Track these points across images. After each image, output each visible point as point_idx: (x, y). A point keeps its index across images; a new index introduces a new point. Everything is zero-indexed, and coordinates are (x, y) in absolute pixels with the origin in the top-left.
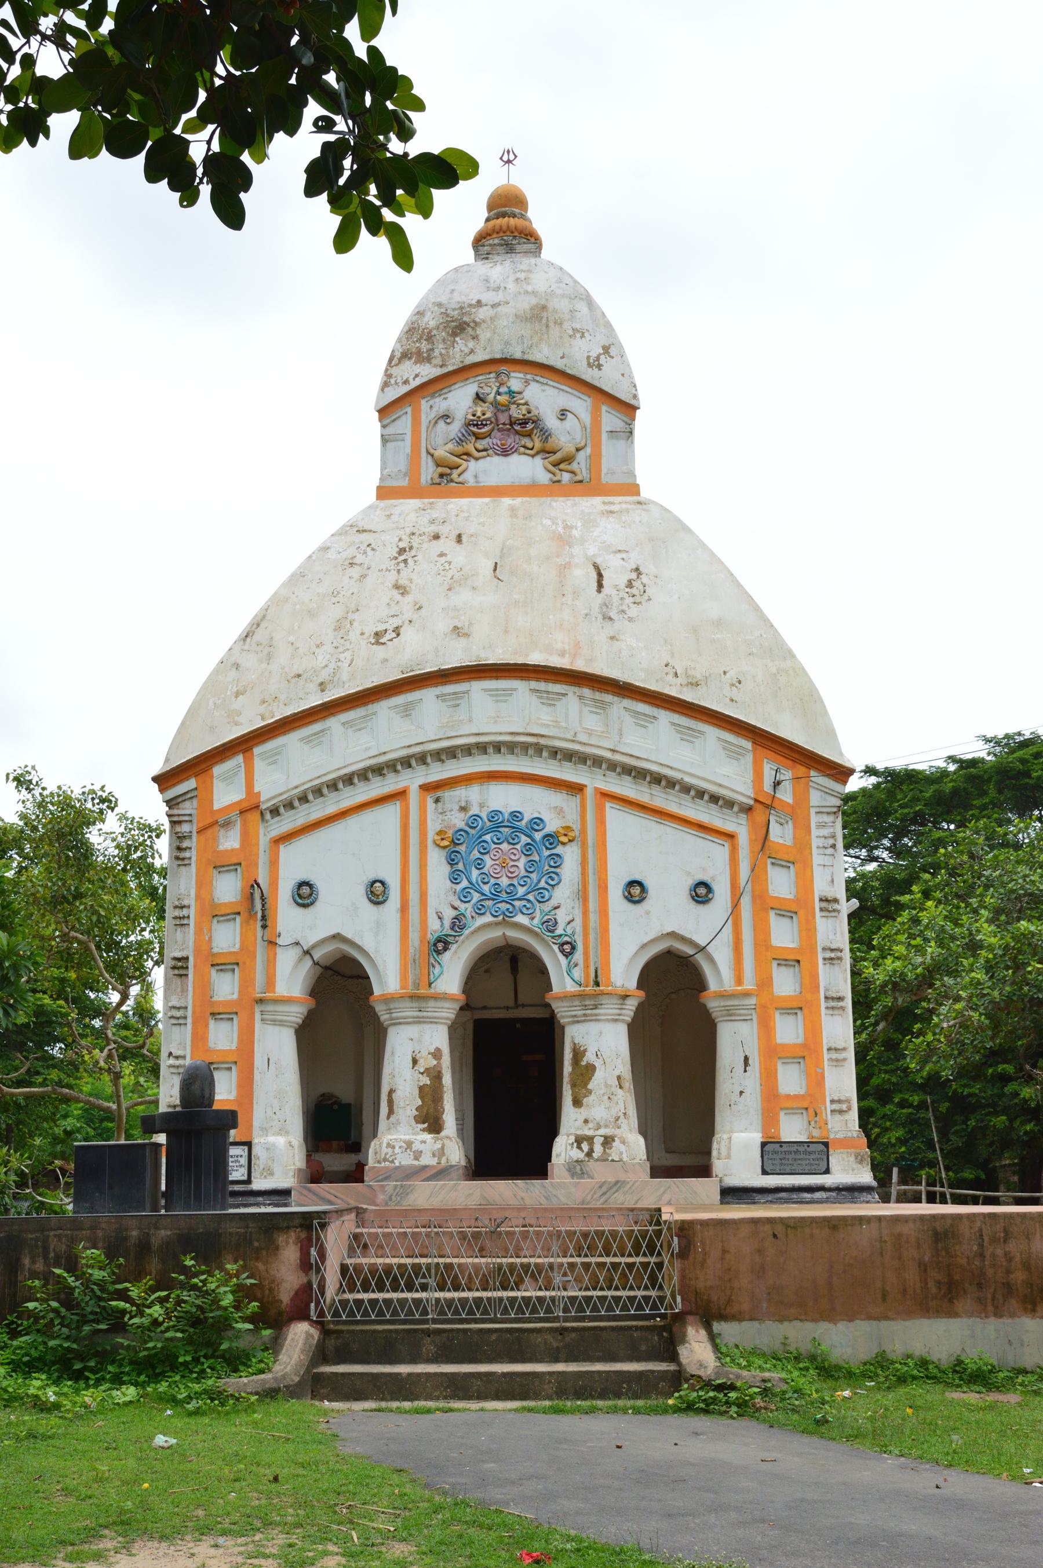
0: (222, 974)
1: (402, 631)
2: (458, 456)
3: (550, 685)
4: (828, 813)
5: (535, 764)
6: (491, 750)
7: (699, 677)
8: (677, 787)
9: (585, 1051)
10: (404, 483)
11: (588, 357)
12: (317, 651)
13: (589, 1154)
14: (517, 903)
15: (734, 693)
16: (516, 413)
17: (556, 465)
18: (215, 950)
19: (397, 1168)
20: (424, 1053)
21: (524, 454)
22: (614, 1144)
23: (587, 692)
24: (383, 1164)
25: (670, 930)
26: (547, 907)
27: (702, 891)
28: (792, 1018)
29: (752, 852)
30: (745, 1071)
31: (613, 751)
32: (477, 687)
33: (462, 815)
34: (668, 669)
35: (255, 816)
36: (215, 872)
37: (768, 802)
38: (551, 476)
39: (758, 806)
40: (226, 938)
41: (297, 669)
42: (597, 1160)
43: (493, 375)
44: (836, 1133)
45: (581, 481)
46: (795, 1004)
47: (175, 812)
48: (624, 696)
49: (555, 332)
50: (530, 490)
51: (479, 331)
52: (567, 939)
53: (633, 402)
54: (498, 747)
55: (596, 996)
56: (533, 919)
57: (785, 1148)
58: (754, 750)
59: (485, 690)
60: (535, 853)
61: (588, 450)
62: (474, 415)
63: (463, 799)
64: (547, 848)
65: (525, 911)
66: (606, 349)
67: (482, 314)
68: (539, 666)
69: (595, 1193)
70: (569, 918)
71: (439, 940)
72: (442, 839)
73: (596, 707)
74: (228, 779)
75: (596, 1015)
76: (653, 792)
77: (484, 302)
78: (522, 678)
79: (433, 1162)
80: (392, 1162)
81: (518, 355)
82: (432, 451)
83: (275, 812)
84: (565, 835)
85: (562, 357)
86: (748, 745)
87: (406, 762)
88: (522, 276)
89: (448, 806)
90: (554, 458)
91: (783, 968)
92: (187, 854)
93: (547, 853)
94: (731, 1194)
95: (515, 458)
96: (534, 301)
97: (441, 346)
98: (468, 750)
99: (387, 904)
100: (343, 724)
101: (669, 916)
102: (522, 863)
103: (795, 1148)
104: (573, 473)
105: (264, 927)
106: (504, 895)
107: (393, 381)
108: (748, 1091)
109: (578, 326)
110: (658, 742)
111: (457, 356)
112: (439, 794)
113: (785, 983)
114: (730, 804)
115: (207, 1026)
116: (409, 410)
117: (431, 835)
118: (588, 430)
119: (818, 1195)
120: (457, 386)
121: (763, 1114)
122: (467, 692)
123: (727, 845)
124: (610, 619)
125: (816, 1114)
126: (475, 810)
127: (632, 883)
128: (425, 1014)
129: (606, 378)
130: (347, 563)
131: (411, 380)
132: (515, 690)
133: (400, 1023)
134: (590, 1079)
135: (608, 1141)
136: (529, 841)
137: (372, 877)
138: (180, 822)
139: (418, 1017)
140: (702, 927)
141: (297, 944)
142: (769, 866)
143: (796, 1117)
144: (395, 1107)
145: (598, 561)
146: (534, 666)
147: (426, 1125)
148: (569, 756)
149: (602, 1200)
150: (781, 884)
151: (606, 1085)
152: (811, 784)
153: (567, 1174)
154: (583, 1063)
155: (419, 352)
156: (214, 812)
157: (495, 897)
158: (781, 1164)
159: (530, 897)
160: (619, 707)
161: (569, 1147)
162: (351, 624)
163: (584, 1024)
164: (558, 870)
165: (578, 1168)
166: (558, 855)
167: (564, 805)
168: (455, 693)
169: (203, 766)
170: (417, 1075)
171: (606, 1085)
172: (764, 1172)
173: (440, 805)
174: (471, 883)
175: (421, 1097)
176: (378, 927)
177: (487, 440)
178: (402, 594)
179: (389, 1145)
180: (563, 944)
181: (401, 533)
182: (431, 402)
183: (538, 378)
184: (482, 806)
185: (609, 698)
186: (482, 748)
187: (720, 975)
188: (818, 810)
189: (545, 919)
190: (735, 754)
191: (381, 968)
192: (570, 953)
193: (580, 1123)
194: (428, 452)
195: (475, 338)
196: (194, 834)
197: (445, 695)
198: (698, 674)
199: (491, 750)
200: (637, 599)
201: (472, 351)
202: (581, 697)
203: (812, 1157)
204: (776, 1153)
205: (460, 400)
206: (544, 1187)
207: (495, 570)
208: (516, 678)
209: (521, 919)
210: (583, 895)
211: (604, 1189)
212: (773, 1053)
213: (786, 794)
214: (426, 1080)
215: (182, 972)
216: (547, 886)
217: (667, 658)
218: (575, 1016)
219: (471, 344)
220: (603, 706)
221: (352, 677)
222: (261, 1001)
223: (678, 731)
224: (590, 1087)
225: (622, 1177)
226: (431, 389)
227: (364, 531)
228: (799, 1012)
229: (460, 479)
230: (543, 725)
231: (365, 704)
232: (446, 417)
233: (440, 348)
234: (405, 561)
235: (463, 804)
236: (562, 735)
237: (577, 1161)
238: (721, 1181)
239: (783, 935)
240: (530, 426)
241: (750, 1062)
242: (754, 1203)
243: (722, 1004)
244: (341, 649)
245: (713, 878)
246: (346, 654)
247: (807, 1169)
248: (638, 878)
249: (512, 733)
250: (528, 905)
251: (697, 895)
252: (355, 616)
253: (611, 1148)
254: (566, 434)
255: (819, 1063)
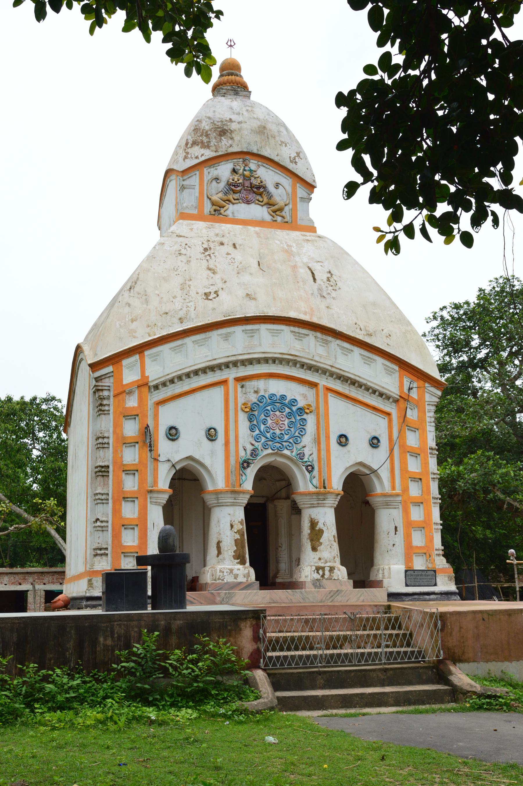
0: (127, 476)
1: (219, 293)
2: (224, 201)
3: (301, 329)
4: (432, 405)
5: (292, 371)
6: (270, 362)
7: (371, 331)
8: (363, 387)
9: (318, 522)
10: (195, 212)
11: (290, 157)
12: (174, 300)
13: (323, 576)
14: (284, 444)
15: (388, 341)
16: (255, 182)
17: (275, 212)
18: (124, 463)
19: (226, 583)
20: (237, 522)
21: (258, 204)
22: (335, 571)
23: (319, 335)
24: (218, 581)
25: (360, 461)
26: (299, 446)
27: (375, 441)
28: (417, 508)
29: (399, 423)
30: (396, 534)
31: (332, 366)
32: (264, 328)
33: (255, 395)
34: (357, 326)
35: (145, 389)
36: (124, 419)
37: (406, 398)
38: (272, 217)
39: (401, 400)
40: (131, 456)
41: (164, 309)
42: (327, 579)
43: (241, 160)
44: (439, 565)
45: (287, 222)
46: (420, 501)
47: (100, 384)
48: (337, 338)
49: (272, 141)
50: (260, 223)
51: (233, 135)
52: (309, 463)
53: (313, 184)
54: (274, 360)
55: (325, 494)
56: (292, 452)
57: (416, 573)
58: (399, 371)
59: (267, 329)
60: (293, 418)
61: (290, 206)
62: (233, 180)
63: (256, 387)
64: (299, 415)
65: (288, 448)
66: (298, 154)
67: (234, 126)
68: (296, 319)
69: (327, 596)
70: (311, 453)
71: (245, 461)
72: (246, 408)
73: (323, 343)
74: (131, 367)
75: (324, 504)
76: (351, 389)
77: (233, 120)
78: (287, 325)
79: (244, 580)
80: (223, 580)
81: (255, 151)
82: (210, 197)
83: (156, 387)
84: (308, 409)
85: (277, 155)
86: (396, 368)
87: (227, 365)
88: (250, 109)
89: (248, 390)
90: (273, 208)
91: (413, 482)
92: (106, 408)
93: (299, 418)
94: (392, 596)
95: (253, 206)
96: (259, 123)
97: (214, 140)
98: (259, 361)
99: (217, 441)
100: (193, 342)
101: (358, 453)
102: (286, 422)
103: (420, 573)
104: (283, 217)
105: (151, 451)
106: (278, 439)
107: (189, 156)
108: (397, 544)
109: (283, 140)
110: (353, 363)
111: (224, 147)
112: (243, 383)
113: (414, 490)
114: (388, 398)
115: (121, 504)
116: (198, 173)
117: (240, 405)
118: (290, 196)
119: (432, 597)
120: (223, 163)
121: (405, 556)
122: (258, 330)
123: (386, 418)
124: (324, 297)
125: (430, 556)
126: (262, 393)
127: (341, 436)
128: (237, 501)
129: (299, 169)
130: (177, 253)
131: (199, 156)
132: (283, 330)
133: (223, 506)
134: (321, 537)
135: (332, 569)
136: (290, 411)
137: (209, 426)
138: (102, 390)
139: (234, 503)
140: (375, 459)
141: (169, 460)
142: (407, 430)
143: (420, 557)
144: (222, 551)
145: (310, 265)
146: (294, 319)
147: (239, 560)
148: (310, 368)
149: (330, 600)
151: (329, 540)
152: (426, 390)
153: (312, 587)
154: (317, 529)
155: (202, 142)
156: (123, 386)
157: (273, 439)
158: (414, 581)
159: (291, 440)
160: (335, 343)
161: (313, 572)
162: (190, 287)
163: (317, 508)
164: (304, 427)
165: (318, 583)
166: (305, 419)
167: (307, 393)
168: (252, 330)
169: (117, 359)
170: (233, 534)
171: (329, 540)
172: (407, 585)
173: (244, 389)
174: (260, 432)
175: (236, 545)
176: (213, 453)
177: (238, 194)
178: (213, 273)
179: (220, 571)
180: (307, 466)
181: (202, 239)
182: (209, 170)
183: (264, 165)
184: (265, 391)
185: (330, 339)
186: (266, 360)
187: (383, 485)
188: (428, 403)
189: (299, 452)
190: (389, 372)
191: (214, 476)
192: (311, 471)
193: (316, 559)
194: (208, 197)
195: (232, 138)
196: (112, 397)
197: (247, 330)
198: (371, 330)
199: (270, 362)
200: (334, 288)
201: (231, 146)
202: (316, 337)
203: (429, 577)
204: (412, 575)
206: (302, 593)
207: (259, 265)
208: (283, 324)
209: (286, 452)
210: (317, 441)
211: (332, 594)
212: (410, 525)
213: (414, 394)
214: (238, 536)
215: (104, 474)
216: (299, 435)
217: (355, 321)
218: (313, 504)
219: (230, 142)
220: (327, 342)
221: (197, 316)
222: (151, 491)
223: (363, 359)
224: (321, 541)
225: (340, 588)
226: (210, 163)
227: (181, 236)
228: (421, 505)
229: (225, 214)
230: (297, 350)
231: (205, 332)
232: (217, 179)
233: (213, 142)
234: (209, 255)
235: (256, 389)
236: (307, 357)
237: (317, 580)
238: (387, 590)
240: (262, 190)
241: (398, 529)
242: (403, 601)
243: (384, 500)
244: (187, 301)
245: (379, 435)
246: (191, 304)
247: (426, 583)
248: (344, 433)
249: (281, 354)
250: (290, 445)
251: (373, 444)
252: (190, 283)
253: (333, 573)
254: (279, 196)
255: (431, 531)
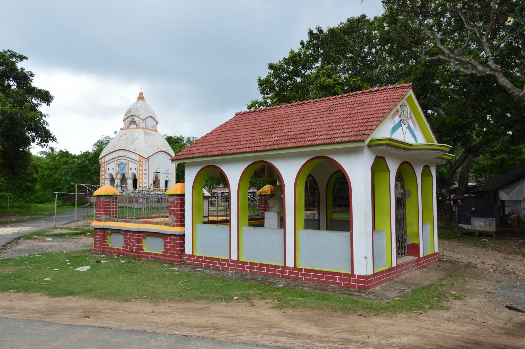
40: (103, 173)
50: (134, 128)
113: (141, 177)
140: (135, 172)
150: (141, 168)
205: (129, 119)
212: (140, 183)
239: (141, 172)
254: (137, 122)
